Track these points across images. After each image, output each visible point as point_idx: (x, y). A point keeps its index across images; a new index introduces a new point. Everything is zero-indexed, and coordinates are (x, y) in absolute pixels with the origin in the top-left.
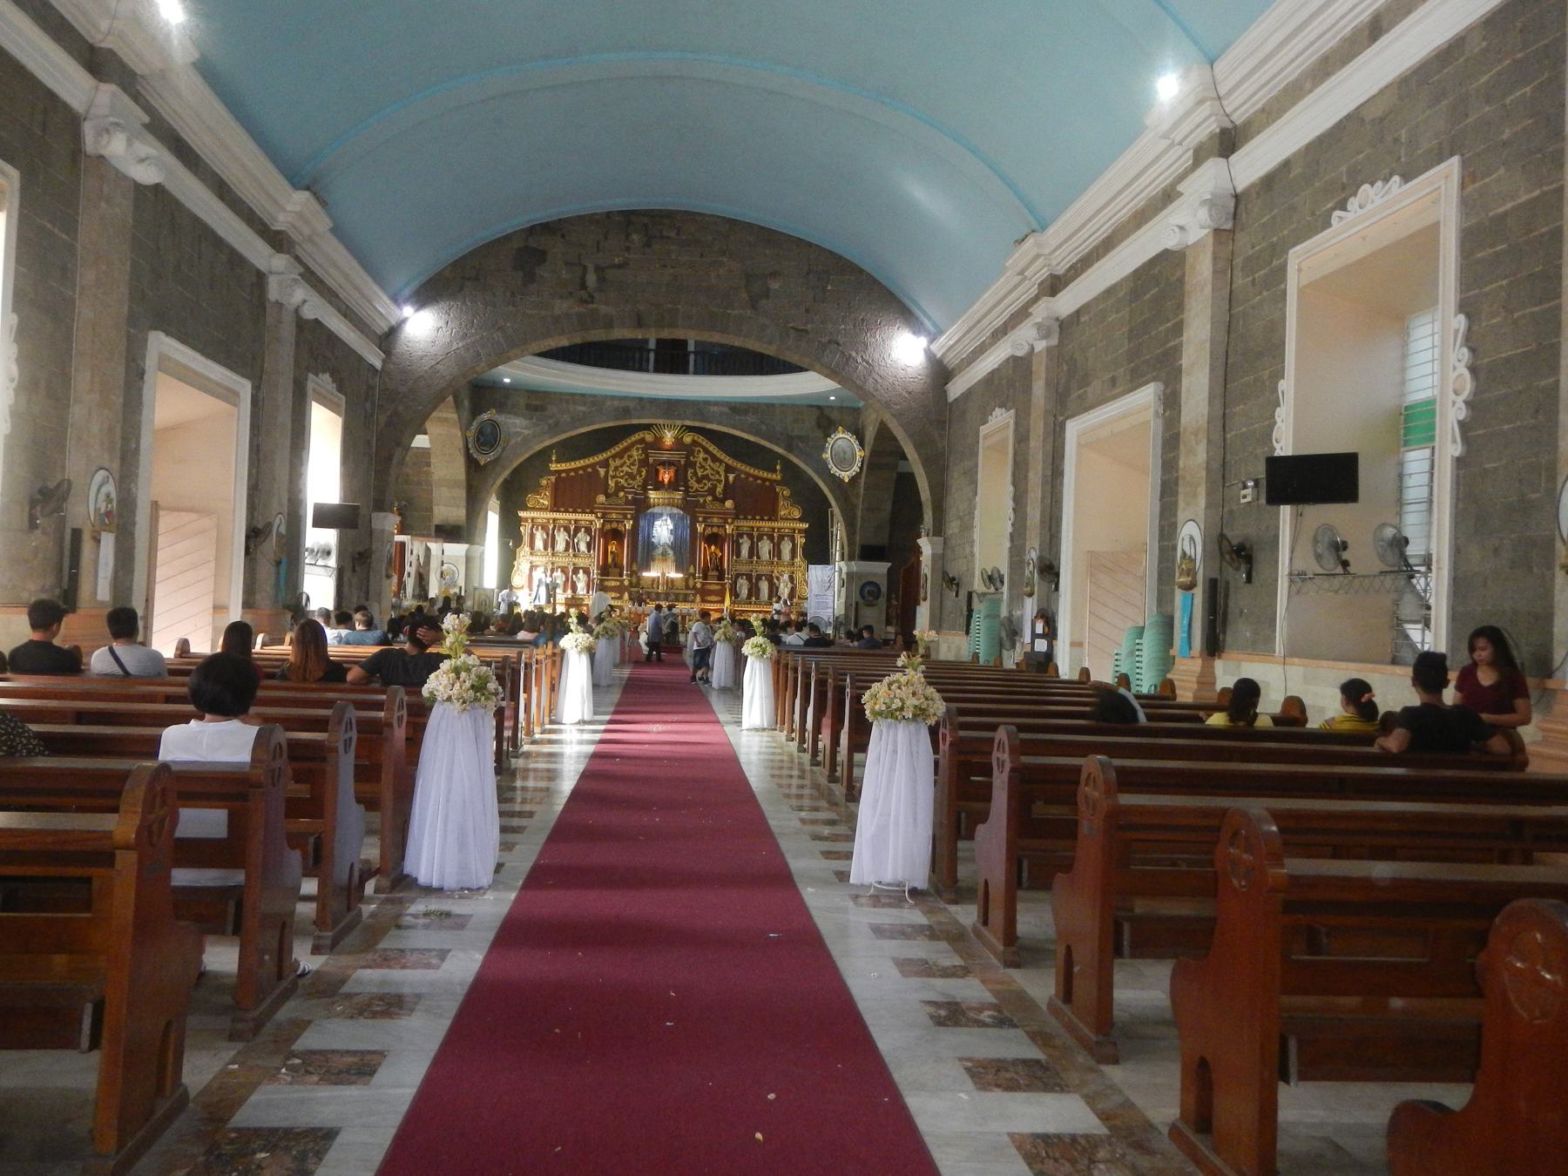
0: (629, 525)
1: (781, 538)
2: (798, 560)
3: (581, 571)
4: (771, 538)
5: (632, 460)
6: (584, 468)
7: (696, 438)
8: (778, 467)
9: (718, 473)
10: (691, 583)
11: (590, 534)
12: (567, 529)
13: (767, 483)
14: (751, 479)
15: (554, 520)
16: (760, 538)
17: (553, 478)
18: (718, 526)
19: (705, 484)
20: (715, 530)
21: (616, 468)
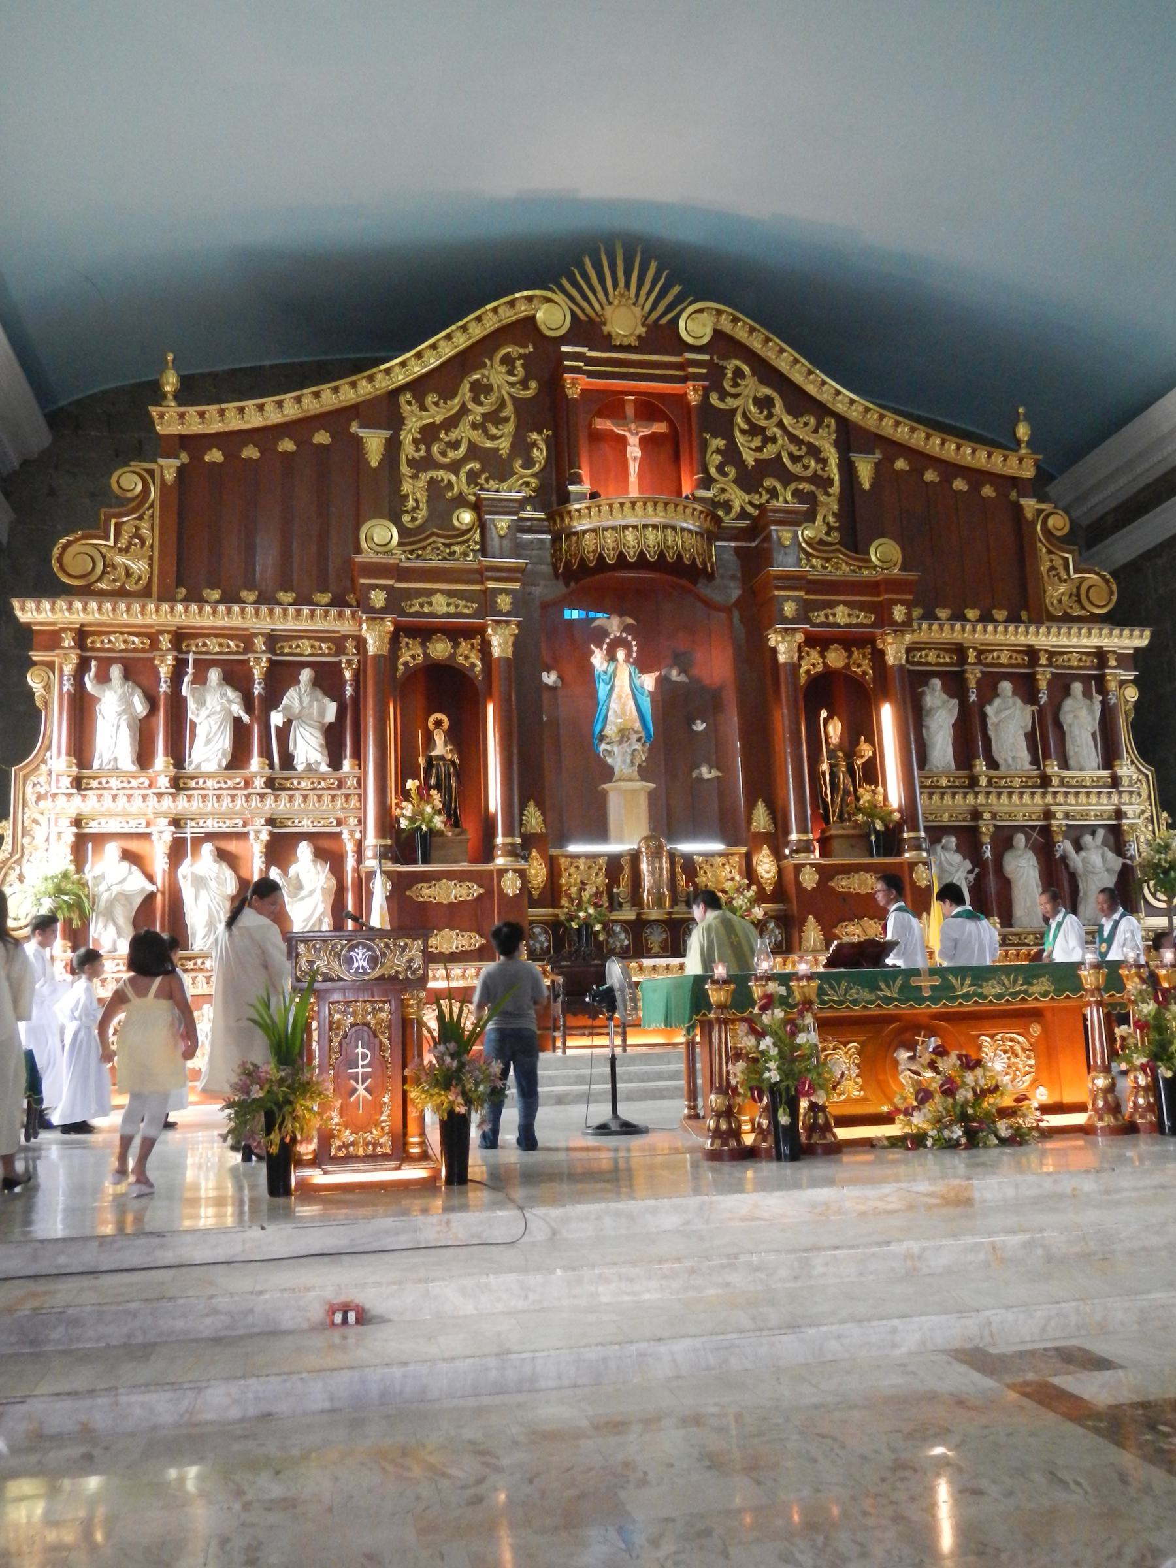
0: (500, 643)
1: (1061, 686)
2: (1126, 770)
3: (304, 850)
4: (1027, 688)
5: (489, 403)
6: (298, 428)
7: (726, 325)
8: (1022, 431)
9: (814, 451)
10: (766, 867)
12: (236, 677)
13: (988, 491)
14: (930, 476)
15: (180, 638)
16: (989, 688)
17: (169, 468)
18: (850, 641)
19: (773, 493)
20: (836, 658)
21: (429, 434)
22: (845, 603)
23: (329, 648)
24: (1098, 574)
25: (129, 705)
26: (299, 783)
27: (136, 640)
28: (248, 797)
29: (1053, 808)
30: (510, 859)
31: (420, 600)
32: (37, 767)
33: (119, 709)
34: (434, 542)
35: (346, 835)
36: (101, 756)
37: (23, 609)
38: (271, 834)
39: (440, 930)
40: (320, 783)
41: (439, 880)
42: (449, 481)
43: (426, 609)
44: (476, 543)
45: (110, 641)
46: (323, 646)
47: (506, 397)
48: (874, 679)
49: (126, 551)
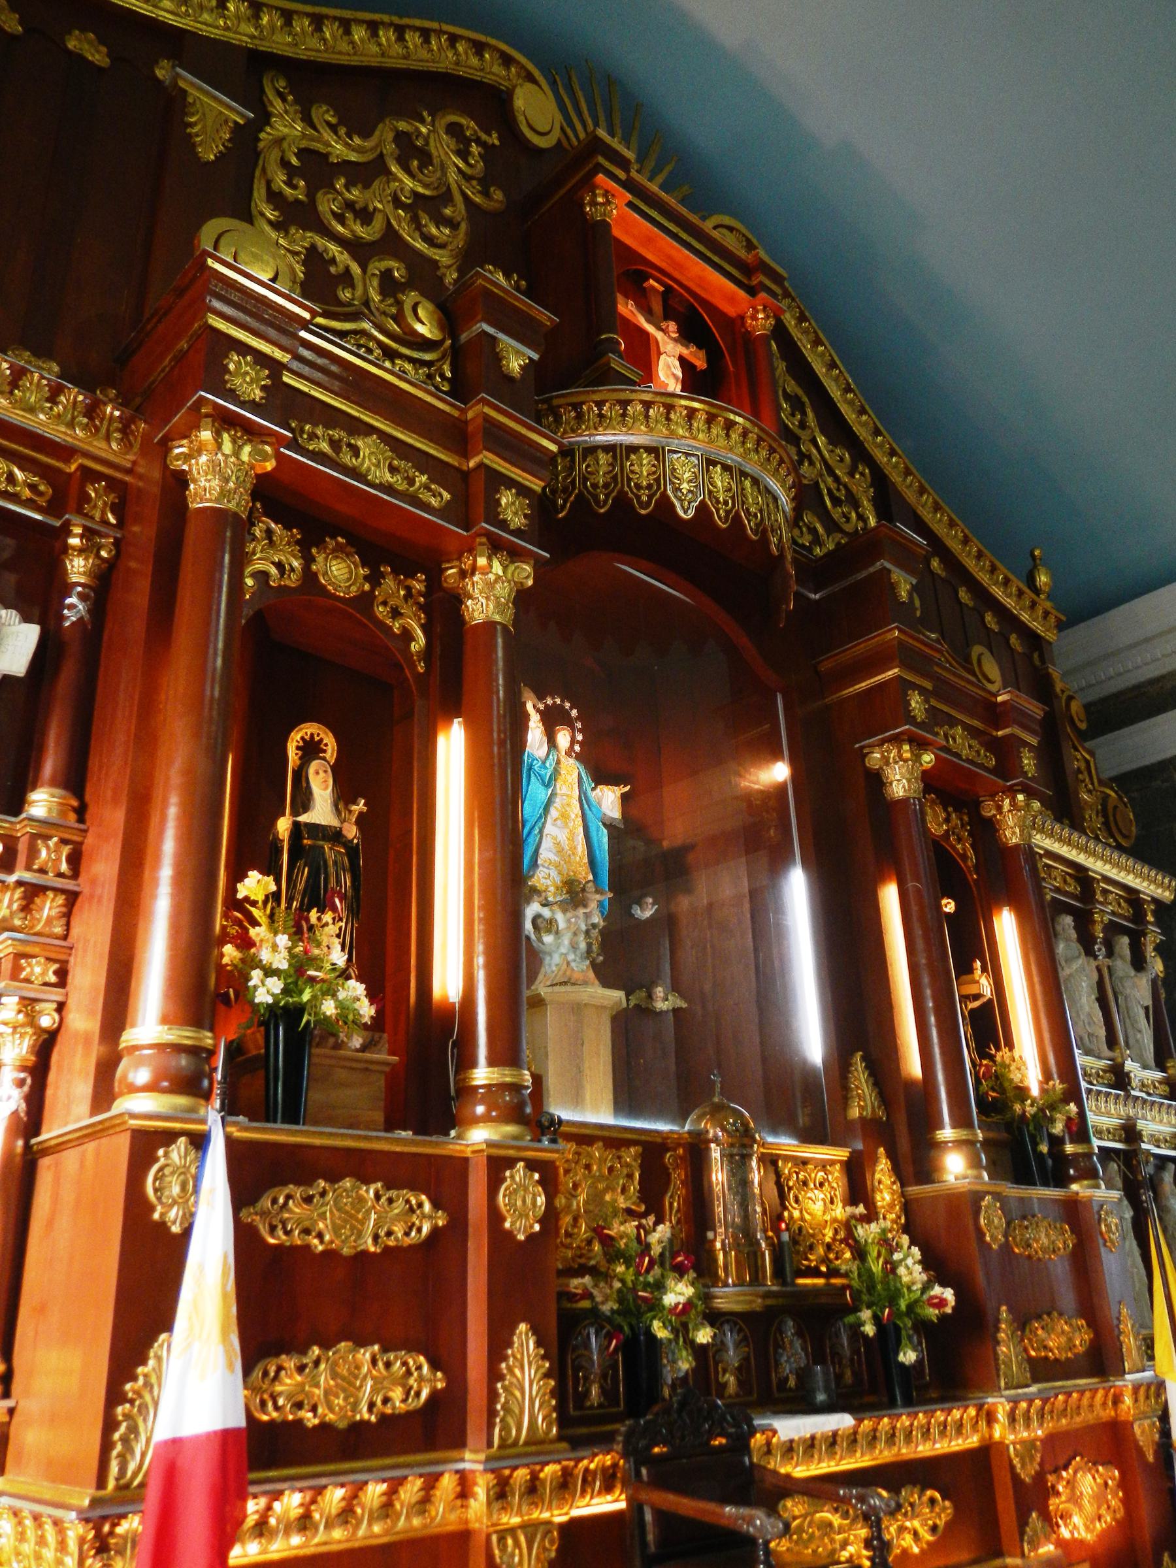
8: (1043, 579)
22: (966, 727)
23: (33, 487)
24: (1116, 792)
29: (1141, 1124)
30: (510, 1129)
31: (336, 434)
34: (363, 333)
39: (326, 1345)
41: (333, 1178)
42: (347, 269)
43: (347, 459)
44: (442, 376)
46: (19, 475)
47: (454, 187)
48: (977, 867)
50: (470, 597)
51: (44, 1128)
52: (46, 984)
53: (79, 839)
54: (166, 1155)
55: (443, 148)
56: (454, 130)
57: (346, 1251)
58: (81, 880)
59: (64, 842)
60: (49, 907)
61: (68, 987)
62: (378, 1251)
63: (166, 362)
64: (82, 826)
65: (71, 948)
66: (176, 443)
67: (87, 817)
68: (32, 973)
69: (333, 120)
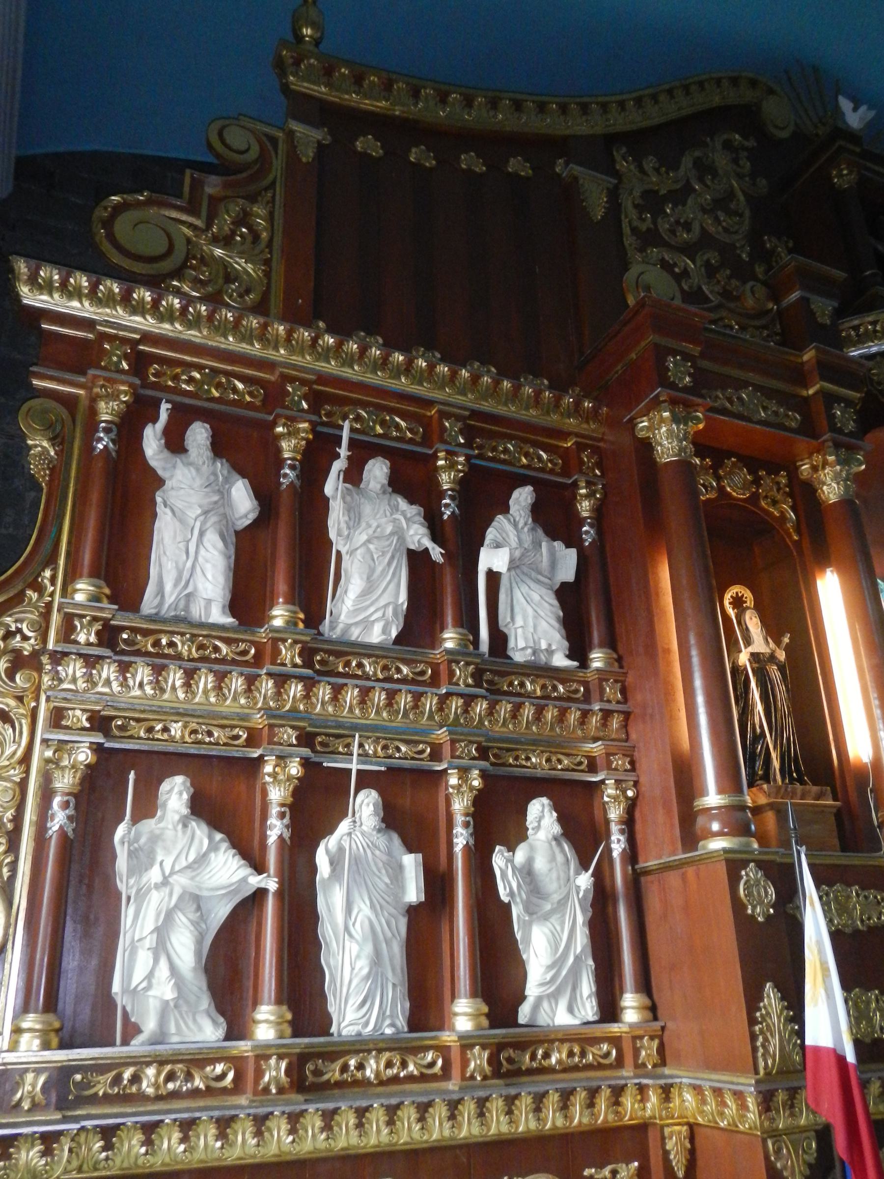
11: (572, 540)
25: (224, 495)
26: (522, 685)
27: (240, 386)
28: (443, 700)
32: (19, 598)
33: (206, 501)
35: (610, 790)
36: (160, 591)
37: (33, 280)
38: (484, 775)
40: (555, 688)
45: (191, 380)
49: (226, 241)
50: (824, 484)
51: (641, 859)
52: (626, 770)
53: (623, 679)
54: (747, 875)
55: (721, 160)
56: (728, 145)
57: (848, 930)
58: (630, 703)
59: (616, 681)
60: (615, 723)
61: (638, 771)
62: (865, 929)
63: (619, 367)
64: (621, 670)
65: (634, 747)
66: (639, 420)
67: (625, 664)
68: (617, 764)
69: (657, 165)
